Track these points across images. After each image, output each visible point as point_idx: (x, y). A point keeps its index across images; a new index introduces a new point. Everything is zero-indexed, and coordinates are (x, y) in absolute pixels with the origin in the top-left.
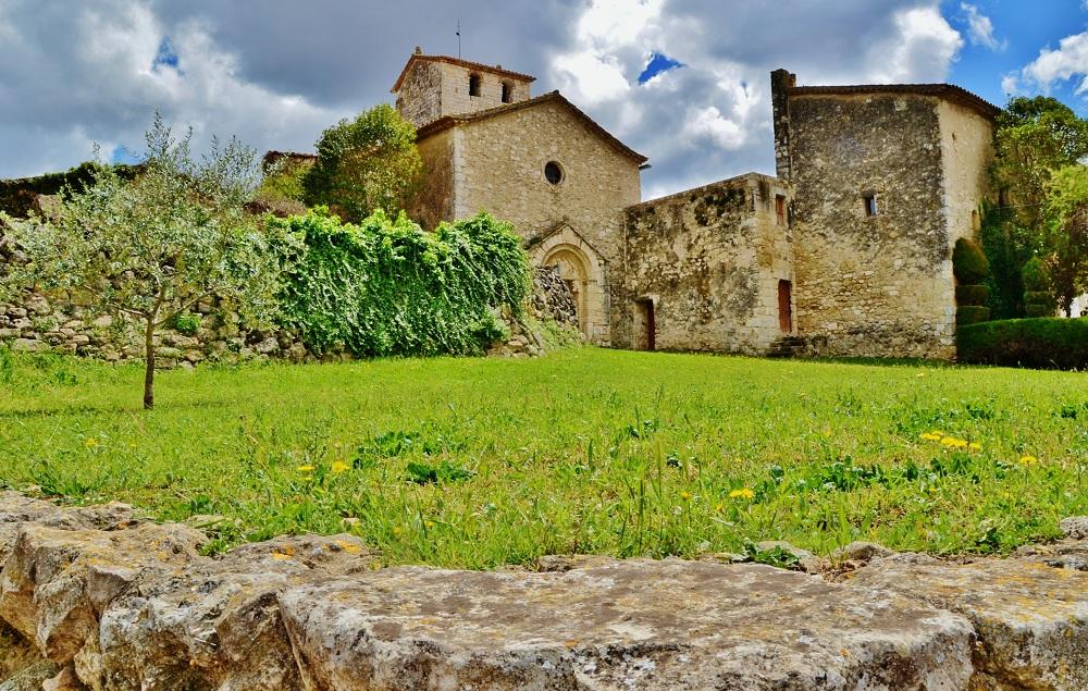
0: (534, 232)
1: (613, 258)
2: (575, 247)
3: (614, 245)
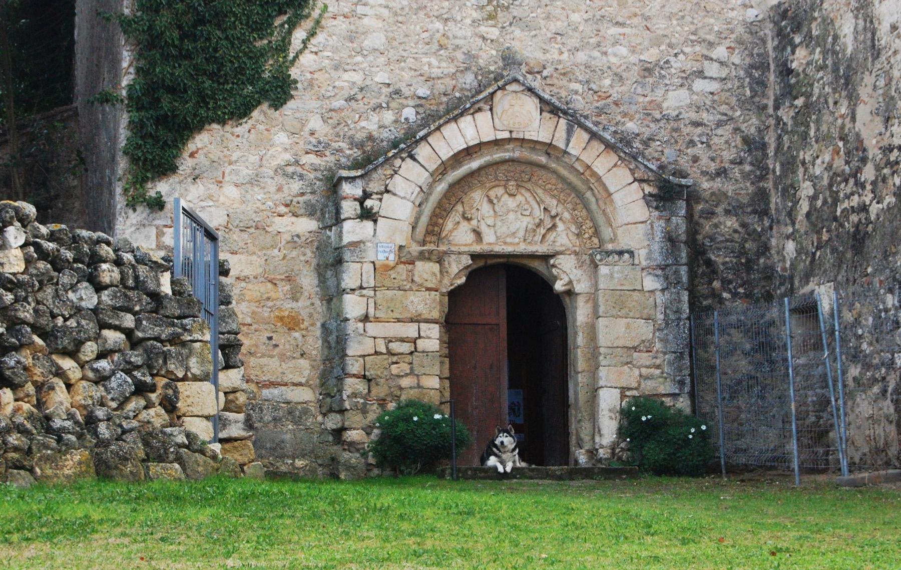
0: (409, 113)
1: (722, 173)
2: (549, 148)
3: (726, 131)
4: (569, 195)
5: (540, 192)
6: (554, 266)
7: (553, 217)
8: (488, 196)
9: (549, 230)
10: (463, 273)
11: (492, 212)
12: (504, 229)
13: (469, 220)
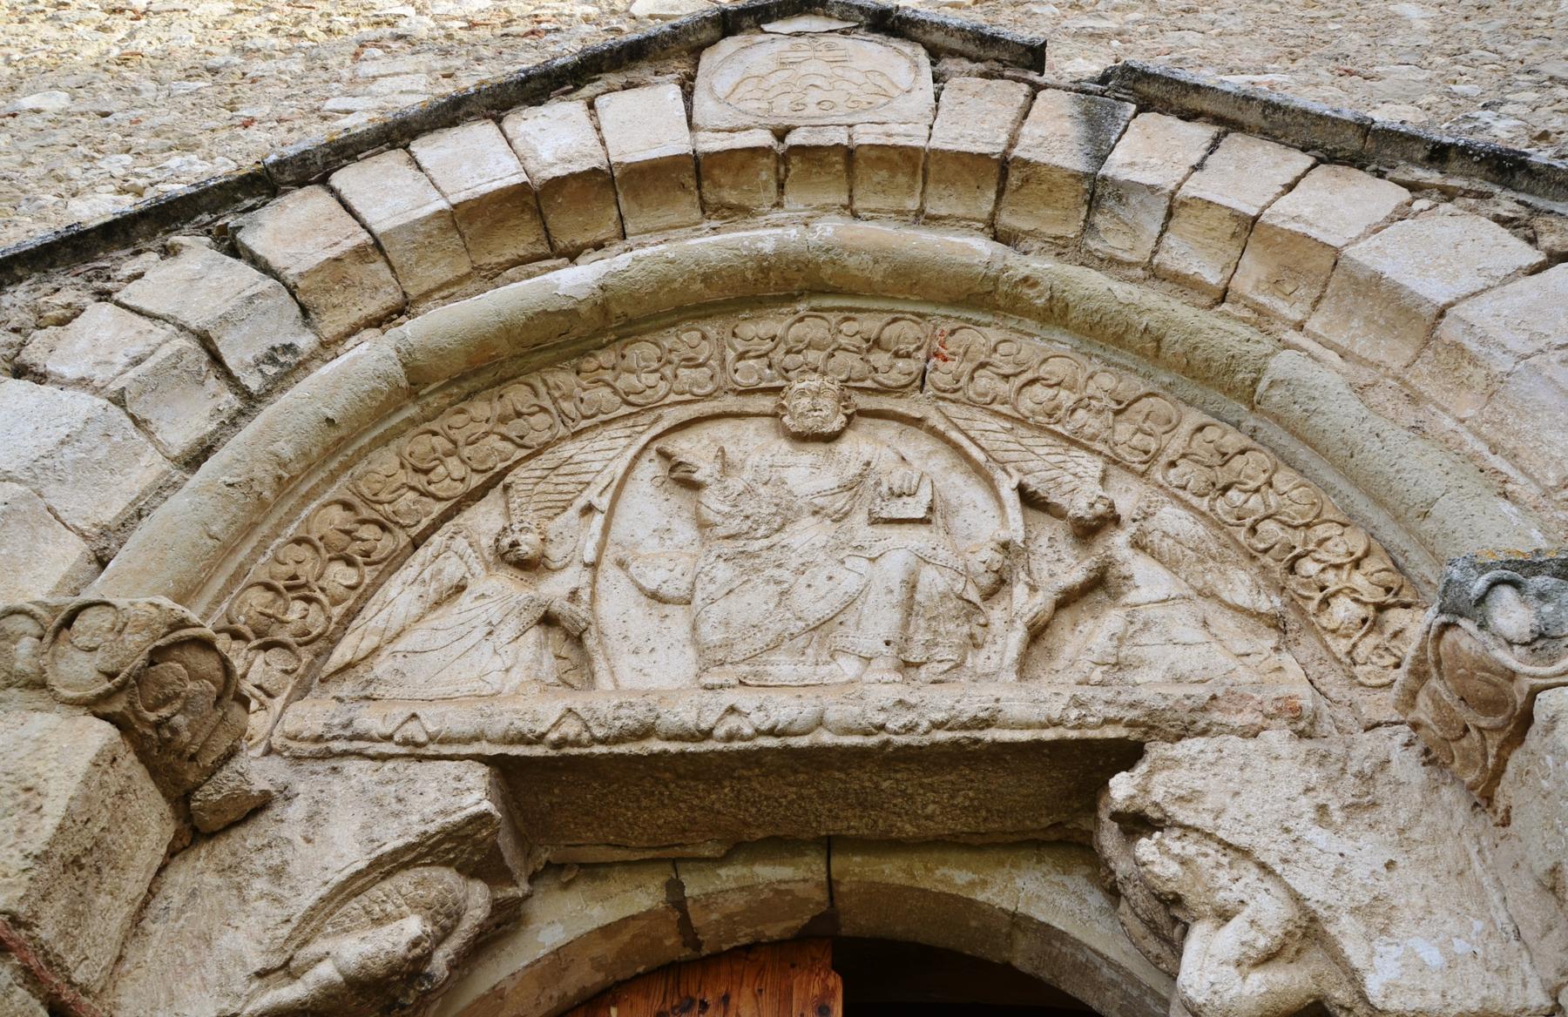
4: (1171, 425)
5: (989, 431)
6: (1137, 824)
7: (1088, 531)
8: (664, 455)
9: (1068, 600)
10: (405, 881)
11: (685, 532)
12: (755, 601)
13: (530, 566)
